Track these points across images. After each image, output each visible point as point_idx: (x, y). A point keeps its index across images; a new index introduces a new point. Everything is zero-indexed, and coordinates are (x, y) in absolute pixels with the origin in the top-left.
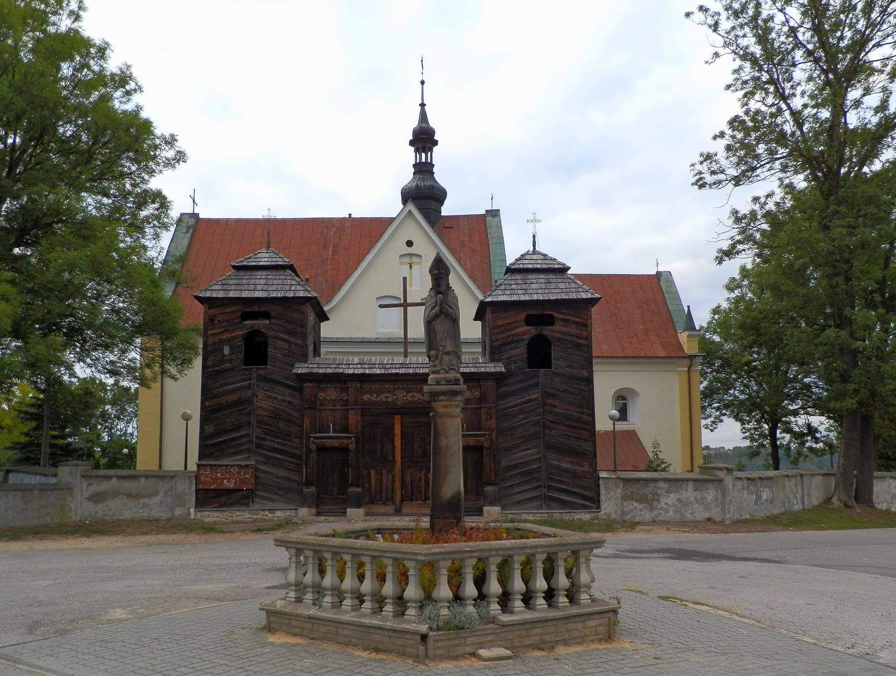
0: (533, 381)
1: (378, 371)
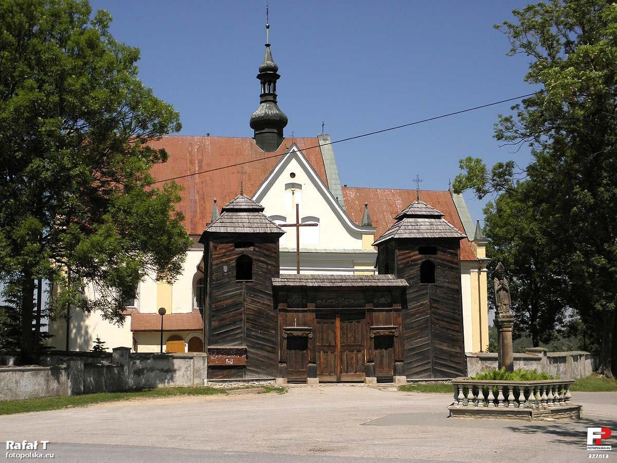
0: (424, 292)
1: (328, 285)
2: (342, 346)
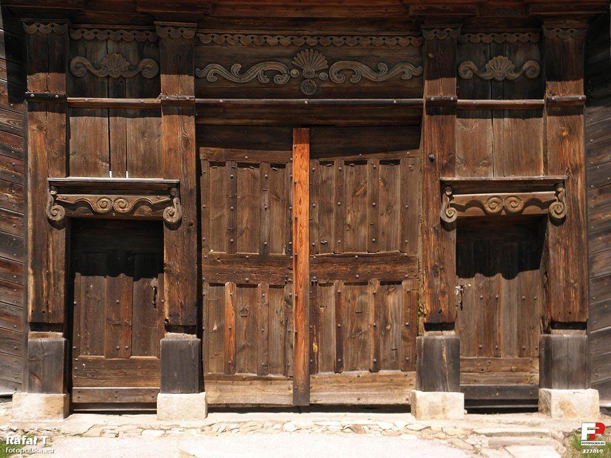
2: (315, 263)
